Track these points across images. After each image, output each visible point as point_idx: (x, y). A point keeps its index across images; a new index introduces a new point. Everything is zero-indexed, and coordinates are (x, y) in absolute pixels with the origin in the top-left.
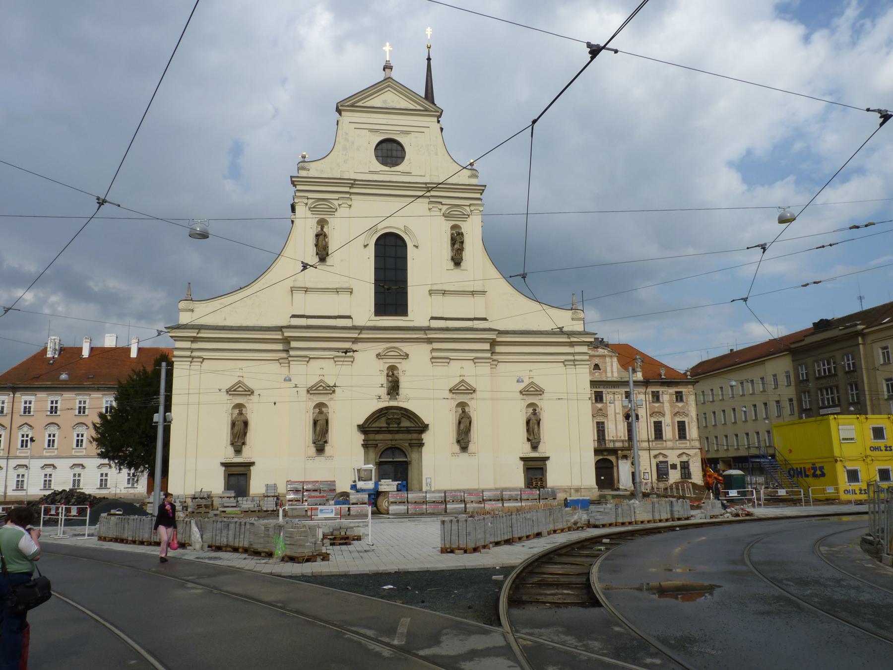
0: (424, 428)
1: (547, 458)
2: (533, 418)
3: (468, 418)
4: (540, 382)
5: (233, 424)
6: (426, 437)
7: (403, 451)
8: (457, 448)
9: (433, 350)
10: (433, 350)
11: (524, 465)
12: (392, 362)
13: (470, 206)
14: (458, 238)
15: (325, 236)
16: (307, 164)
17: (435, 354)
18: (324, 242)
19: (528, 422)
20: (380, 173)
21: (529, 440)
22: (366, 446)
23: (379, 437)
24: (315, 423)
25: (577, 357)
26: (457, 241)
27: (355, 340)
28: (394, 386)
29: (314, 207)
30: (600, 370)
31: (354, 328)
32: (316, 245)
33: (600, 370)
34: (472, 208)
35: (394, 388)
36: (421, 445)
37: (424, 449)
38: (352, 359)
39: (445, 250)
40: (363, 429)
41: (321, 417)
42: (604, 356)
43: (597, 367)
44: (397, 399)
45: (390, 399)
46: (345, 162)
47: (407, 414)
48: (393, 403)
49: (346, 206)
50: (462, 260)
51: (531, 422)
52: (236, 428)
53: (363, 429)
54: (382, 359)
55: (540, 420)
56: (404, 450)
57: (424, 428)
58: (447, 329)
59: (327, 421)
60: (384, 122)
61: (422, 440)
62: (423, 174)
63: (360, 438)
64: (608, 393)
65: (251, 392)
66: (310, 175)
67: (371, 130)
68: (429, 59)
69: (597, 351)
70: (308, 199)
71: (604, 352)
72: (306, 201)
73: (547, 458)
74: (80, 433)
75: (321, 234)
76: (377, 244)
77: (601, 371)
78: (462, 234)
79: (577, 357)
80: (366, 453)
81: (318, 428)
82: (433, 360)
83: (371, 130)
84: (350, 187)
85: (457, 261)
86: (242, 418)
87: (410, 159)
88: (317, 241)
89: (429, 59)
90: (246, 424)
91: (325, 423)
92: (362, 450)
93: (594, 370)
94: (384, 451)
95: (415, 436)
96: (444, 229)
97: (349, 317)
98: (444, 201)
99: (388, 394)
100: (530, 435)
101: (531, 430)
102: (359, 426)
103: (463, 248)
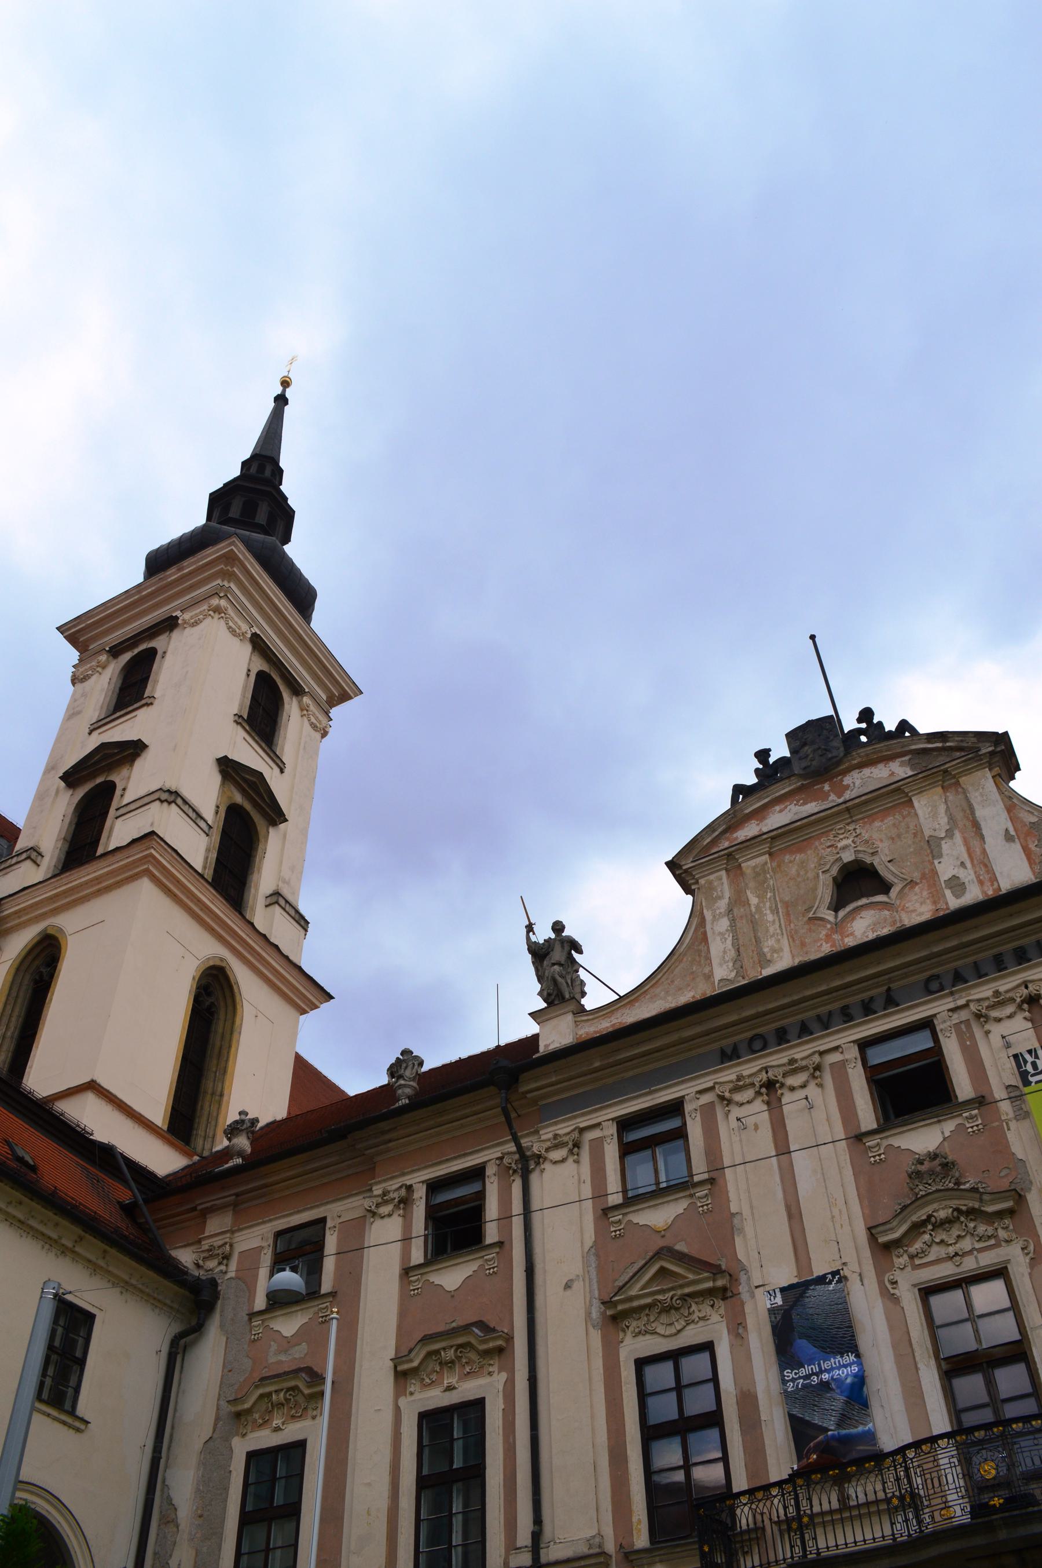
30: (885, 887)
33: (885, 887)
64: (980, 1016)
68: (281, 400)
69: (841, 790)
71: (892, 774)
77: (894, 892)
89: (281, 400)
93: (836, 907)
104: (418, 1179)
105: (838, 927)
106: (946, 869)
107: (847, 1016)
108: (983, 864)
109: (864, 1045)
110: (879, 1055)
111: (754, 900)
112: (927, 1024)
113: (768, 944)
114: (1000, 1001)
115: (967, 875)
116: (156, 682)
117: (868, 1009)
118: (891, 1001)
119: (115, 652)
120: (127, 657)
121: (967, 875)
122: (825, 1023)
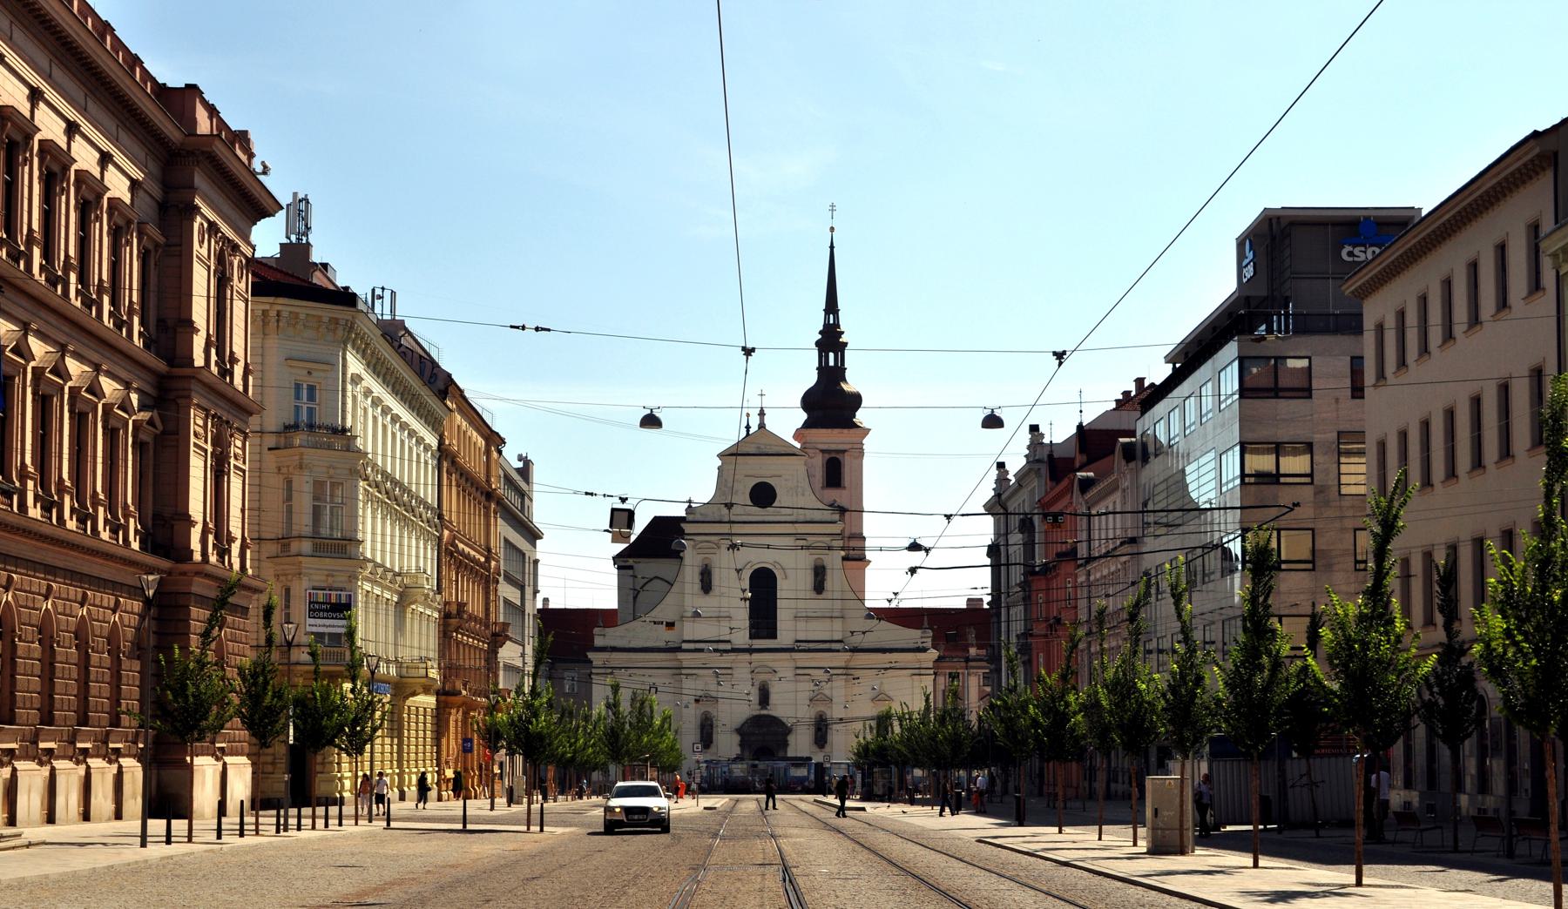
6: (791, 738)
12: (763, 677)
26: (819, 573)
31: (734, 650)
39: (807, 579)
40: (739, 731)
47: (775, 721)
48: (764, 712)
53: (739, 731)
68: (832, 247)
79: (923, 671)
85: (819, 587)
89: (832, 247)
96: (805, 560)
97: (729, 641)
99: (760, 704)
104: (948, 671)
119: (823, 451)
120: (827, 456)
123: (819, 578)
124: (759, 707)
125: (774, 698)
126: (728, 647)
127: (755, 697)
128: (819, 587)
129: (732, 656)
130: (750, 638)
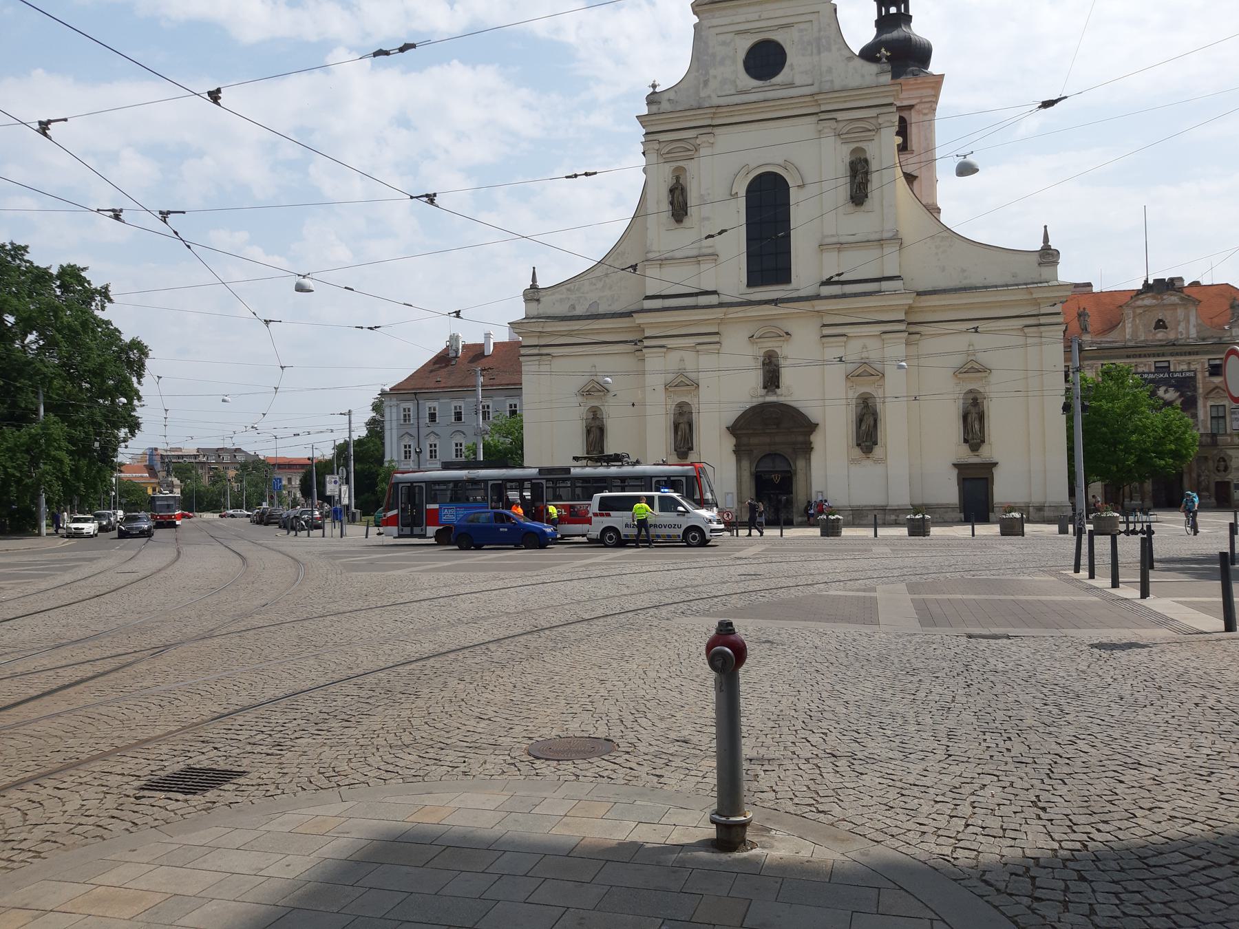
0: (811, 427)
1: (995, 464)
2: (973, 410)
3: (873, 414)
4: (984, 359)
5: (589, 432)
6: (816, 439)
7: (784, 457)
8: (857, 452)
9: (824, 325)
10: (824, 325)
11: (959, 474)
12: (769, 345)
13: (877, 117)
14: (859, 167)
15: (683, 190)
16: (657, 95)
17: (827, 331)
18: (680, 198)
19: (965, 418)
20: (754, 90)
21: (966, 441)
22: (738, 451)
23: (754, 441)
24: (676, 427)
25: (1043, 320)
27: (721, 322)
28: (772, 377)
29: (668, 153)
30: (1167, 328)
31: (721, 305)
32: (672, 203)
34: (880, 121)
35: (772, 379)
36: (807, 449)
37: (815, 457)
38: (717, 346)
41: (684, 419)
42: (1174, 306)
43: (1160, 325)
44: (776, 393)
45: (768, 392)
46: (706, 83)
48: (771, 398)
49: (707, 145)
50: (867, 197)
51: (969, 419)
52: (592, 436)
53: (734, 430)
54: (757, 343)
55: (983, 412)
56: (787, 456)
57: (811, 427)
58: (844, 296)
59: (690, 425)
60: (756, 16)
61: (811, 443)
62: (810, 82)
63: (730, 442)
65: (604, 390)
66: (661, 111)
67: (739, 33)
69: (1163, 300)
70: (660, 142)
72: (656, 146)
73: (995, 464)
74: (459, 442)
75: (677, 188)
76: (748, 191)
78: (866, 161)
79: (1043, 320)
80: (739, 461)
81: (679, 433)
82: (825, 340)
83: (739, 33)
84: (712, 118)
86: (598, 423)
87: (792, 65)
88: (673, 197)
90: (602, 430)
91: (687, 427)
92: (733, 458)
93: (1155, 329)
94: (762, 458)
95: (801, 439)
97: (714, 292)
98: (839, 116)
99: (765, 387)
100: (968, 433)
101: (969, 427)
102: (728, 428)
103: (867, 181)
105: (1155, 334)
106: (1180, 329)
107: (1154, 355)
108: (1188, 332)
109: (1155, 362)
110: (1158, 365)
111: (1138, 321)
112: (1169, 361)
113: (1139, 334)
114: (1183, 361)
115: (1184, 332)
116: (911, 141)
117: (1158, 355)
118: (1163, 355)
121: (1184, 332)
122: (1149, 356)
123: (859, 179)
124: (763, 392)
125: (787, 376)
126: (713, 300)
127: (755, 378)
128: (859, 195)
129: (718, 313)
130: (751, 283)
